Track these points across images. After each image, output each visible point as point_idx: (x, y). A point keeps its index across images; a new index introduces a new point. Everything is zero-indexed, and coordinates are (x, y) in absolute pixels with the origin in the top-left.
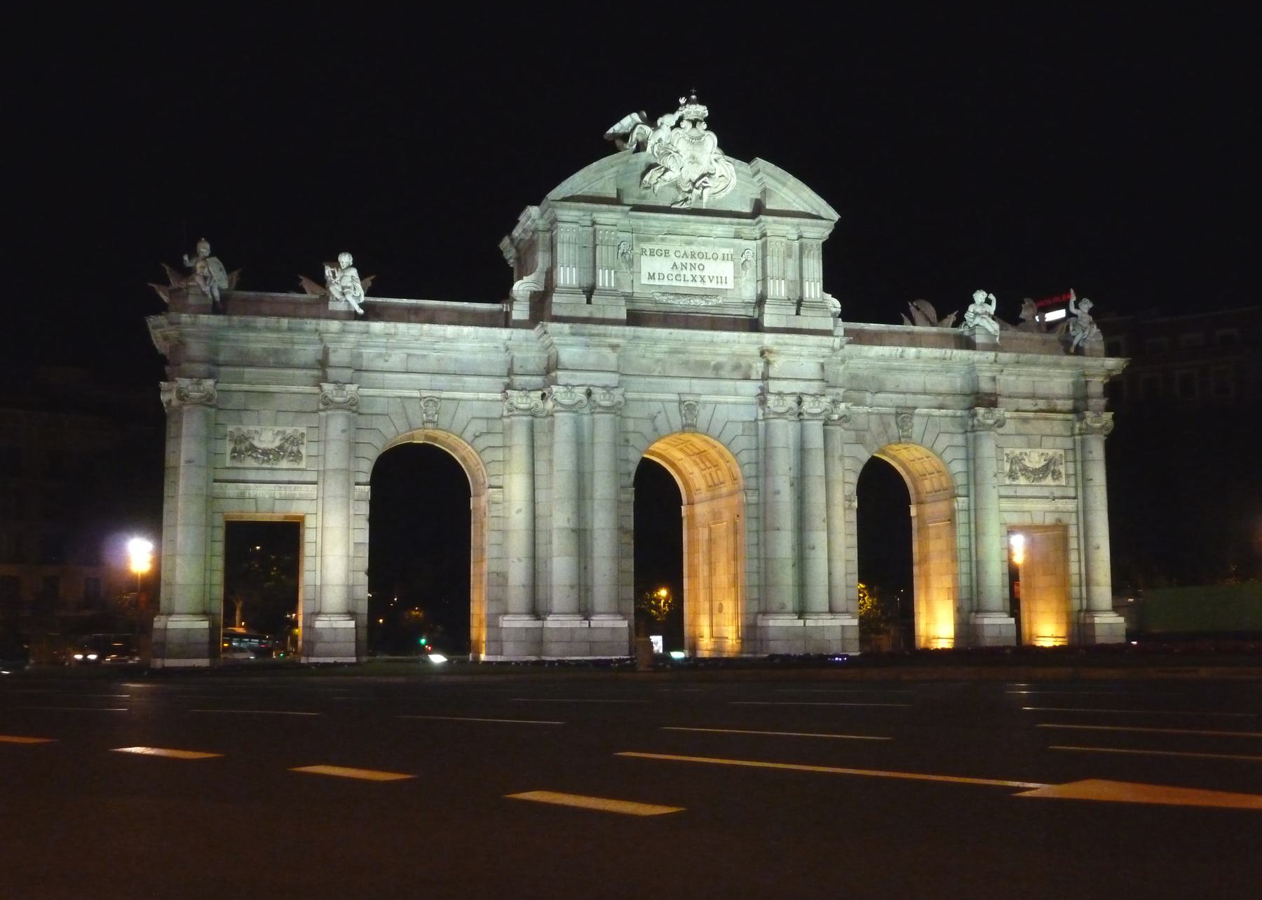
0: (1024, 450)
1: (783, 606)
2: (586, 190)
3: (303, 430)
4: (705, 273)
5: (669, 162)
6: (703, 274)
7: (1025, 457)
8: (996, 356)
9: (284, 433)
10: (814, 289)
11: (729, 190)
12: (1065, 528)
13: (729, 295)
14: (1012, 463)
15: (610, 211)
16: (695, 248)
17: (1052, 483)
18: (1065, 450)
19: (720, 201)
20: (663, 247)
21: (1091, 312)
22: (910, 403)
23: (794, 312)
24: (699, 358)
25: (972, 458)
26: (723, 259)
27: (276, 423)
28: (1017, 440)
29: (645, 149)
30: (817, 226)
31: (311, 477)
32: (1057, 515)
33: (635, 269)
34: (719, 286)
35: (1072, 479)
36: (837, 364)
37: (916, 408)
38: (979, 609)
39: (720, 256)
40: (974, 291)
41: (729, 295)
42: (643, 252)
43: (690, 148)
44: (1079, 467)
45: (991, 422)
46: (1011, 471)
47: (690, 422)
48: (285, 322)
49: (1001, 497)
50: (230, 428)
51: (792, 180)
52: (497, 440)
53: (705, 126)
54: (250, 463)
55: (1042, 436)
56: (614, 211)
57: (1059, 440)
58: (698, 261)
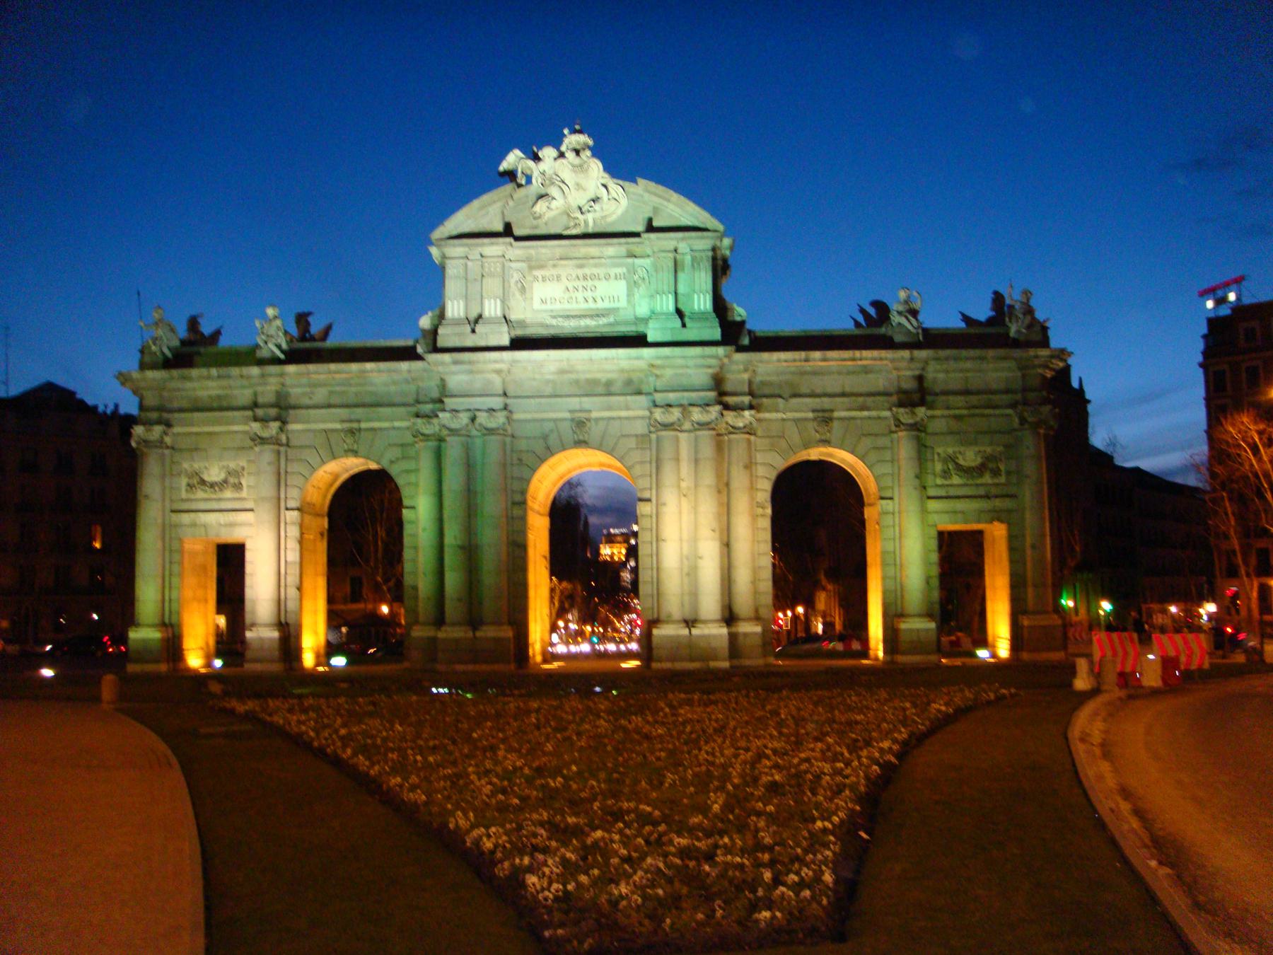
0: (957, 449)
1: (670, 615)
3: (243, 463)
4: (597, 294)
5: (554, 191)
7: (958, 455)
8: (911, 353)
11: (619, 212)
16: (587, 271)
17: (990, 481)
19: (613, 223)
20: (554, 272)
22: (827, 406)
24: (589, 376)
26: (616, 278)
27: (221, 459)
29: (534, 181)
30: (702, 238)
33: (528, 295)
36: (739, 372)
37: (832, 411)
38: (902, 615)
39: (613, 275)
42: (536, 278)
43: (574, 175)
47: (581, 438)
48: (214, 371)
49: (929, 498)
50: (186, 465)
51: (675, 196)
52: (411, 465)
53: (588, 153)
54: (200, 494)
55: (980, 433)
56: (497, 244)
58: (590, 283)
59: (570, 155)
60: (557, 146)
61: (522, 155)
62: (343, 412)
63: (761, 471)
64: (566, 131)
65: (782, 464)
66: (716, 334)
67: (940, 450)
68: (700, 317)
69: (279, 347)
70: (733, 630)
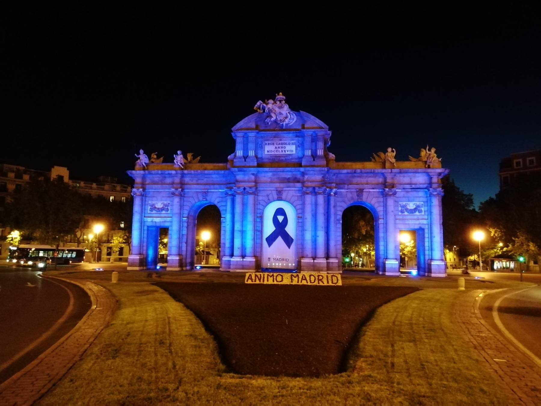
1: (307, 255)
2: (245, 126)
4: (286, 149)
6: (285, 149)
7: (407, 205)
9: (164, 203)
10: (320, 152)
12: (423, 230)
13: (294, 155)
14: (402, 207)
15: (252, 132)
16: (282, 142)
18: (424, 202)
21: (435, 152)
23: (313, 160)
25: (385, 206)
27: (162, 200)
28: (404, 199)
31: (170, 215)
32: (420, 225)
34: (291, 153)
35: (426, 213)
37: (364, 189)
39: (291, 143)
40: (387, 148)
41: (294, 155)
42: (266, 144)
44: (429, 208)
45: (391, 193)
46: (401, 210)
50: (150, 202)
53: (284, 102)
54: (154, 212)
57: (421, 199)
58: (284, 146)
59: (278, 103)
60: (274, 100)
61: (262, 102)
62: (202, 187)
63: (339, 208)
64: (277, 95)
65: (345, 206)
66: (325, 162)
67: (400, 203)
68: (320, 157)
69: (181, 164)
70: (329, 261)
